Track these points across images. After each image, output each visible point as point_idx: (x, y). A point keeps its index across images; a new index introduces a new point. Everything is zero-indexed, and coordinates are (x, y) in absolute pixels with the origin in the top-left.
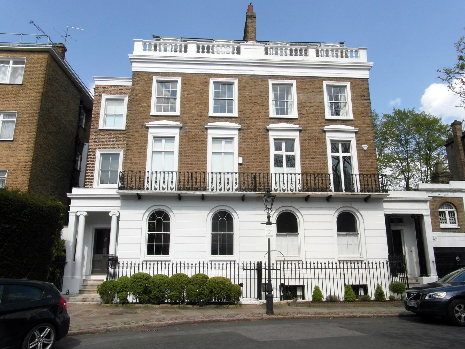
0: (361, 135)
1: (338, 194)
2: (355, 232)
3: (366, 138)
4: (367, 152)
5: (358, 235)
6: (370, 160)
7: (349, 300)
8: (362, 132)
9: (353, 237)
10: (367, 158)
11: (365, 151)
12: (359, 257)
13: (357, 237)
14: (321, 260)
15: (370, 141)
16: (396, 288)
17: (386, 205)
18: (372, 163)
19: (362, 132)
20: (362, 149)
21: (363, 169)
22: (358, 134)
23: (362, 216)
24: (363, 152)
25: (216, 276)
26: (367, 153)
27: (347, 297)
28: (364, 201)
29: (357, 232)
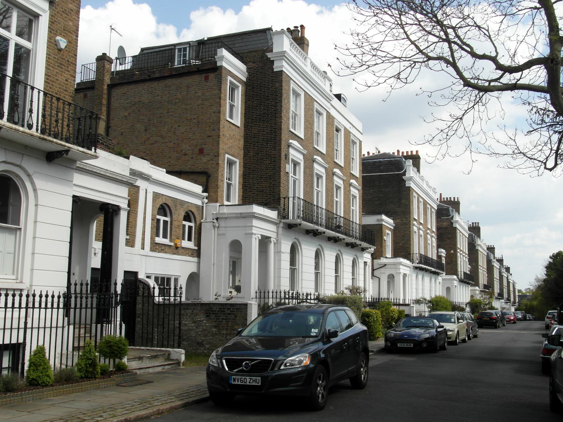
0: (58, 12)
1: (15, 130)
2: (7, 224)
3: (65, 23)
4: (63, 55)
5: (18, 233)
6: (65, 73)
7: (44, 382)
8: (62, 8)
9: (7, 235)
10: (61, 68)
11: (60, 50)
12: (15, 281)
13: (13, 237)
14: (53, 289)
15: (70, 32)
16: (117, 348)
17: (79, 178)
18: (67, 83)
19: (62, 8)
20: (56, 44)
21: (51, 88)
22: (54, 8)
23: (35, 190)
24: (57, 51)
25: (12, 342)
26: (63, 57)
27: (39, 377)
28: (45, 159)
29: (19, 225)
